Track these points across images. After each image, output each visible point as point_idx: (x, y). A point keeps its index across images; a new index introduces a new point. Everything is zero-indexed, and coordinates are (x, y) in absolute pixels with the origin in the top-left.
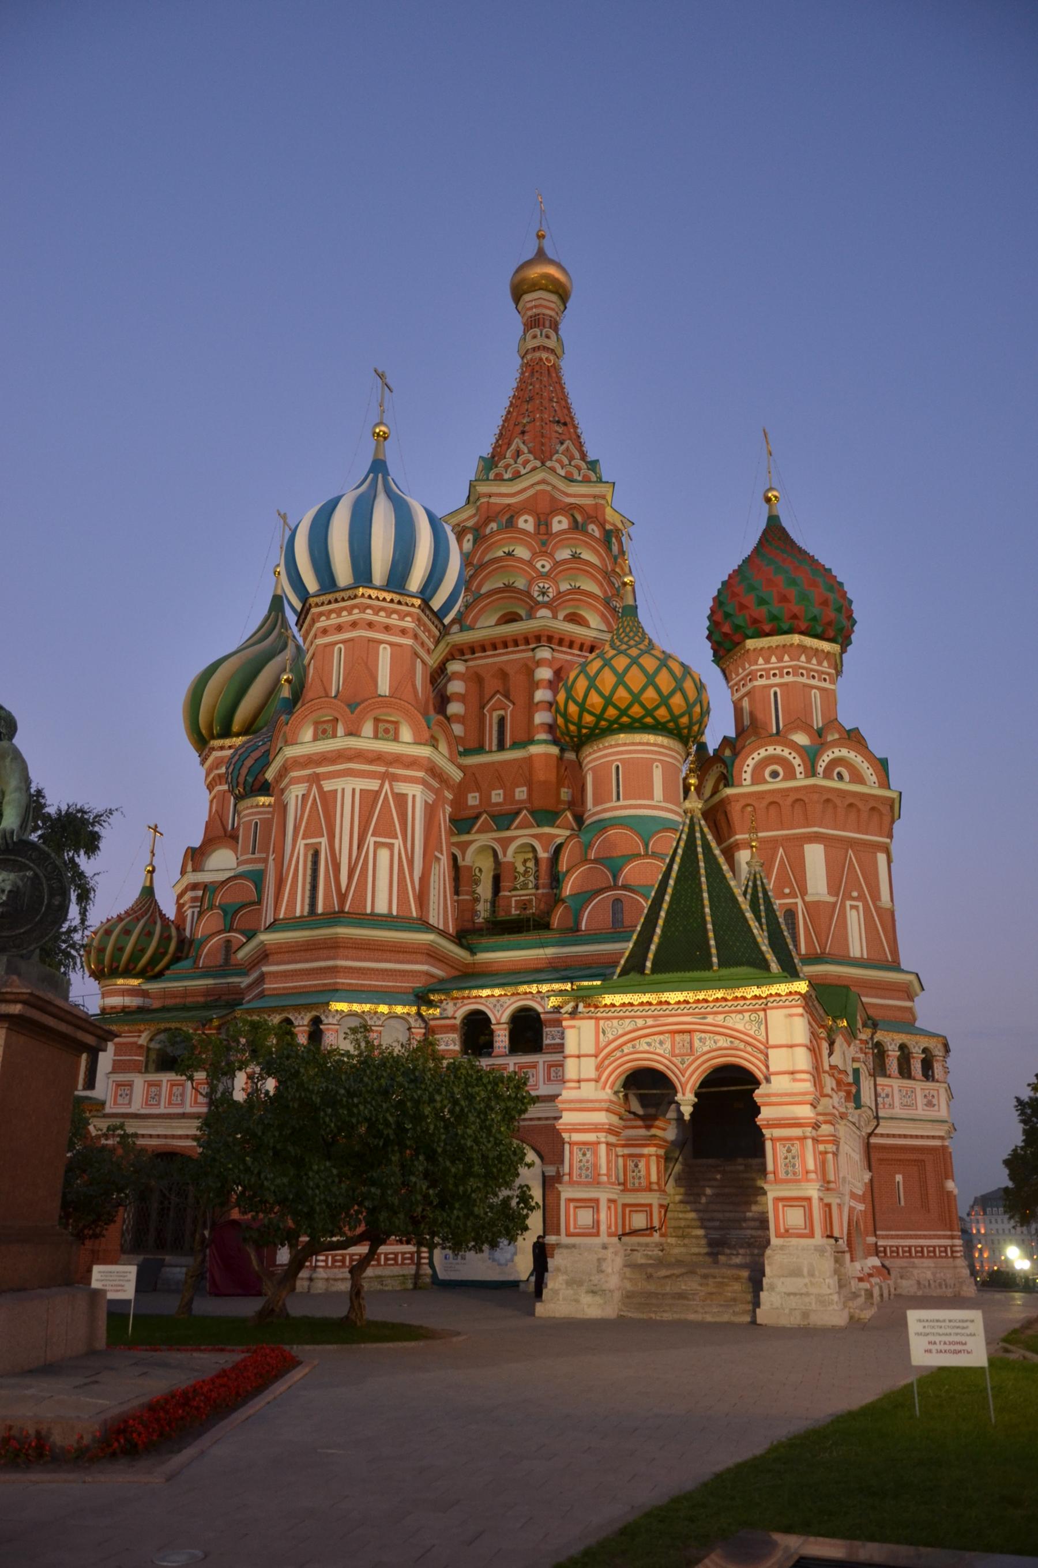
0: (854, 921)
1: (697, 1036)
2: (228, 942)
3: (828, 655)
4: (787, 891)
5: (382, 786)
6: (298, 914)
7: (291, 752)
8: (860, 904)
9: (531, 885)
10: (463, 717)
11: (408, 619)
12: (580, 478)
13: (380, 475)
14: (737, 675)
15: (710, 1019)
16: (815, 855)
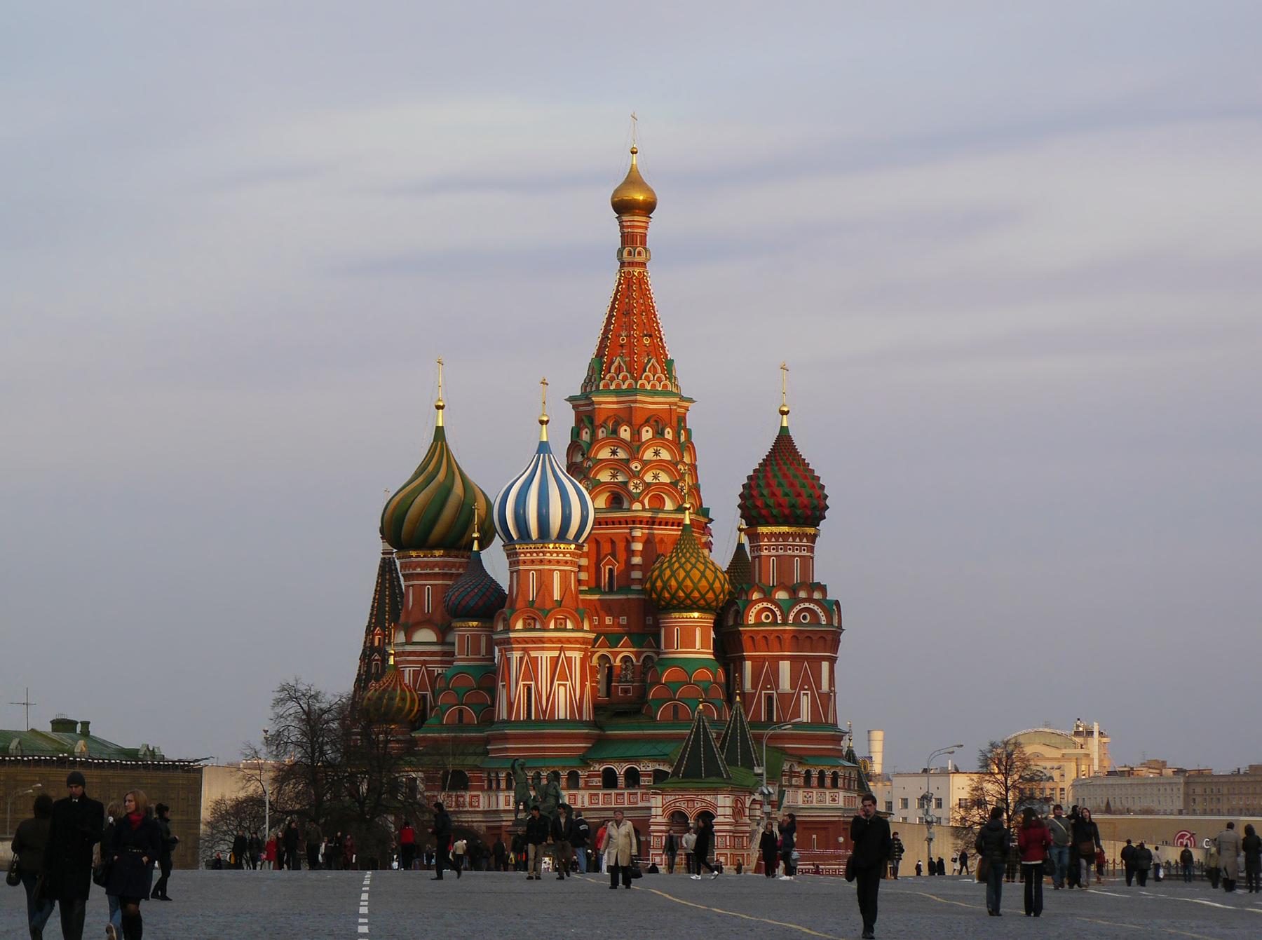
0: (805, 703)
1: (695, 802)
2: (461, 711)
3: (806, 535)
4: (769, 686)
5: (560, 654)
6: (522, 719)
7: (512, 635)
8: (809, 692)
9: (628, 678)
10: (587, 566)
11: (568, 555)
12: (660, 389)
13: (546, 455)
14: (754, 543)
15: (700, 797)
16: (785, 667)
